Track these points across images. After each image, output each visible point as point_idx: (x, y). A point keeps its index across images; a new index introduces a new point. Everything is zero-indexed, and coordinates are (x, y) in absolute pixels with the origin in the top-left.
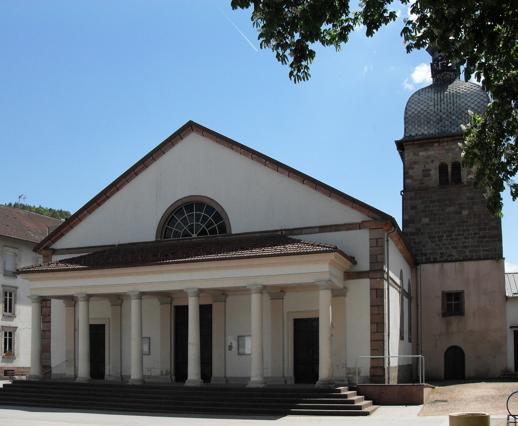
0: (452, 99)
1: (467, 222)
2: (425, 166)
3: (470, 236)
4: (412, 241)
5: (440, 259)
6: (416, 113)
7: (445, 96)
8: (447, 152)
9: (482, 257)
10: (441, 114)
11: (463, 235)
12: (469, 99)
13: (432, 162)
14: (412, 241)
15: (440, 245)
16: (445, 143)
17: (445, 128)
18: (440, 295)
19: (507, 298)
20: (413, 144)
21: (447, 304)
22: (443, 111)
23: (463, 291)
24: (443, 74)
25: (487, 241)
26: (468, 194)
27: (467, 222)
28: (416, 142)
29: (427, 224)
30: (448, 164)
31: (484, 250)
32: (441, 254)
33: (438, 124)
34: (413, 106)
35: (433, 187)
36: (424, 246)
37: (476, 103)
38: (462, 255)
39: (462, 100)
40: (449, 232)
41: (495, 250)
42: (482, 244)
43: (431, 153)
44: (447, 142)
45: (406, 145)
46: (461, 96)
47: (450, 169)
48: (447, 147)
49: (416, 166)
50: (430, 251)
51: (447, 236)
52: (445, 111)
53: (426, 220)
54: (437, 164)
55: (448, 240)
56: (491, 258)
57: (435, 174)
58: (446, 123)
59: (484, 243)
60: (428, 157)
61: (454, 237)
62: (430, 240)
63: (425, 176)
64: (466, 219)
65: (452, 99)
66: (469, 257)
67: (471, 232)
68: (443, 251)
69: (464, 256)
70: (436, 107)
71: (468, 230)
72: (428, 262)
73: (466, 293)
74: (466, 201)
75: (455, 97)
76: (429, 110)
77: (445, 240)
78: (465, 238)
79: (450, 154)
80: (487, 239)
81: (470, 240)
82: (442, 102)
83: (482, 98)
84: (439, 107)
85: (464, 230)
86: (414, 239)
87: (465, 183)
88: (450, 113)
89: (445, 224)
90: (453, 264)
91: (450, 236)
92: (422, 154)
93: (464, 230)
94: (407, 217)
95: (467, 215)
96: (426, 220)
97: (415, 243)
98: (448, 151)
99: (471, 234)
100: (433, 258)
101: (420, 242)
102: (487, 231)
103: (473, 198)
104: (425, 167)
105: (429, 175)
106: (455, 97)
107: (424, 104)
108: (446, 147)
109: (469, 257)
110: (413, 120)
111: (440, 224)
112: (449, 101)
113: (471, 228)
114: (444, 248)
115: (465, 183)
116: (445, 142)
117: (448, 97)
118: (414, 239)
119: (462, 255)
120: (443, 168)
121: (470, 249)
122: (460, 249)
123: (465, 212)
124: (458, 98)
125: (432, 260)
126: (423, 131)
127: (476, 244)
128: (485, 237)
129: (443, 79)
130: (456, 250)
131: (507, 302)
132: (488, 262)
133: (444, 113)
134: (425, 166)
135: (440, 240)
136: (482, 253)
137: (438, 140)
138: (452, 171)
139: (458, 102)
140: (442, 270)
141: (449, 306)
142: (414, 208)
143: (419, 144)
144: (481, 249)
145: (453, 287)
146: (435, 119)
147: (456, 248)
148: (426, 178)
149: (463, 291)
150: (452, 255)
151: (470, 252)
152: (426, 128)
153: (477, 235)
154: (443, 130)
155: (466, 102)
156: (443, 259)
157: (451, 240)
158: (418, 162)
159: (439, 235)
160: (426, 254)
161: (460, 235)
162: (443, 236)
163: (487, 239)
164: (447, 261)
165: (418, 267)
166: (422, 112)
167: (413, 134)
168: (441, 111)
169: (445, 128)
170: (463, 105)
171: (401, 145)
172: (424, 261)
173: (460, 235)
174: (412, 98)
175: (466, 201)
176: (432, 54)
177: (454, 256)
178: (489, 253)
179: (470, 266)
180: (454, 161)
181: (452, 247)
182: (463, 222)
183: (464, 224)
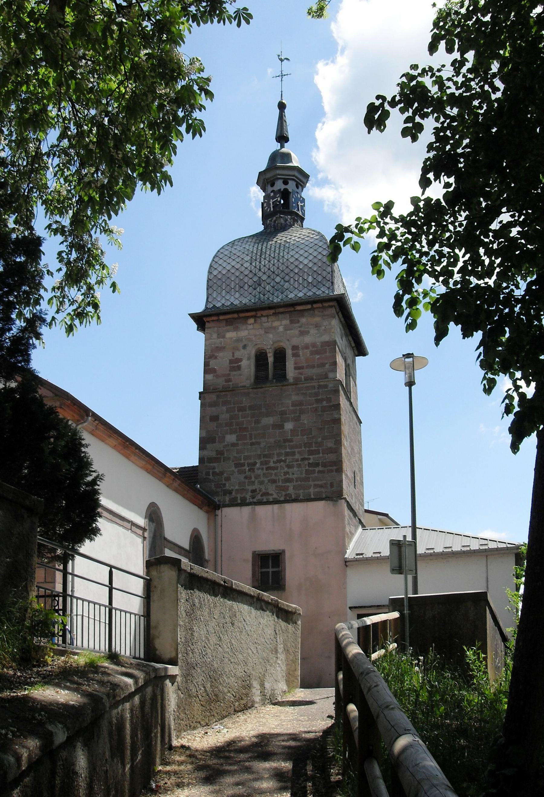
0: (277, 252)
1: (291, 441)
2: (233, 353)
3: (295, 463)
4: (211, 471)
5: (251, 500)
6: (224, 272)
7: (269, 247)
8: (266, 332)
9: (312, 497)
10: (260, 274)
11: (285, 461)
12: (301, 252)
13: (245, 347)
14: (211, 471)
15: (251, 478)
16: (264, 319)
17: (264, 295)
18: (250, 557)
19: (346, 562)
20: (218, 320)
21: (269, 572)
22: (262, 270)
23: (284, 551)
24: (275, 218)
25: (319, 472)
26: (295, 398)
27: (291, 441)
28: (221, 317)
29: (233, 445)
30: (268, 351)
31: (316, 486)
32: (253, 491)
33: (255, 289)
34: (220, 262)
35: (245, 386)
36: (228, 479)
37: (311, 257)
38: (284, 493)
39: (291, 253)
40: (265, 456)
41: (332, 485)
42: (313, 475)
43: (243, 333)
44: (267, 316)
45: (208, 322)
46: (292, 247)
47: (271, 360)
48: (266, 325)
49: (221, 354)
50: (237, 487)
51: (262, 463)
52: (266, 270)
53: (231, 438)
54: (252, 351)
55: (262, 469)
56: (327, 499)
57: (248, 366)
58: (267, 288)
59: (316, 475)
60: (239, 340)
61: (272, 464)
62: (236, 470)
63: (232, 369)
64: (289, 437)
65: (277, 252)
66: (293, 497)
67: (297, 456)
68: (256, 486)
69: (286, 495)
70: (254, 264)
71: (293, 454)
72: (233, 504)
73: (287, 555)
74: (291, 408)
75: (282, 248)
76: (243, 269)
77: (258, 469)
78: (289, 466)
79: (271, 336)
80: (320, 468)
81: (295, 469)
82: (263, 256)
83: (320, 250)
84: (258, 263)
85: (287, 454)
86: (214, 468)
87: (291, 380)
88: (274, 272)
89: (259, 443)
90: (269, 507)
91: (267, 463)
92: (231, 335)
93: (287, 454)
94: (204, 435)
95: (291, 430)
96: (231, 438)
97: (214, 474)
98: (267, 331)
99: (297, 460)
100: (241, 498)
101: (222, 473)
102: (321, 455)
103: (300, 404)
104: (233, 356)
105: (239, 368)
106: (282, 248)
107: (237, 260)
108: (264, 324)
109: (293, 497)
110: (219, 283)
111: (252, 444)
112: (272, 255)
113: (297, 450)
114: (256, 482)
115: (291, 380)
116: (264, 316)
117: (273, 249)
118: (214, 468)
119: (284, 493)
120: (260, 358)
121: (295, 483)
122: (280, 484)
123: (289, 426)
124: (286, 250)
125: (239, 501)
126: (232, 299)
127: (304, 475)
128: (317, 465)
129: (274, 225)
130: (274, 485)
131: (348, 569)
132: (320, 504)
133: (264, 273)
134: (233, 353)
135: (252, 470)
136: (312, 490)
137: (253, 313)
138: (275, 362)
139: (286, 257)
140: (253, 518)
141: (264, 575)
142: (215, 418)
143: (226, 320)
144: (311, 483)
145: (269, 544)
146: (250, 282)
147: (274, 481)
148: (235, 373)
149: (284, 551)
150: (267, 494)
151: (295, 488)
152: (237, 295)
153: (306, 462)
154: (262, 299)
155: (297, 256)
156: (255, 500)
157: (267, 469)
158: (224, 348)
159: (250, 461)
160: (230, 492)
161: (281, 461)
162: (255, 464)
163: (320, 468)
164: (260, 503)
165: (218, 512)
166: (233, 271)
167: (218, 305)
168: (260, 270)
169: (264, 295)
170: (292, 260)
171: (201, 320)
172: (227, 503)
173: (281, 461)
174: (221, 251)
175: (291, 408)
176: (264, 189)
177: (272, 495)
178: (323, 490)
179: (295, 511)
180: (276, 345)
181: (269, 481)
182: (286, 441)
183: (287, 444)
